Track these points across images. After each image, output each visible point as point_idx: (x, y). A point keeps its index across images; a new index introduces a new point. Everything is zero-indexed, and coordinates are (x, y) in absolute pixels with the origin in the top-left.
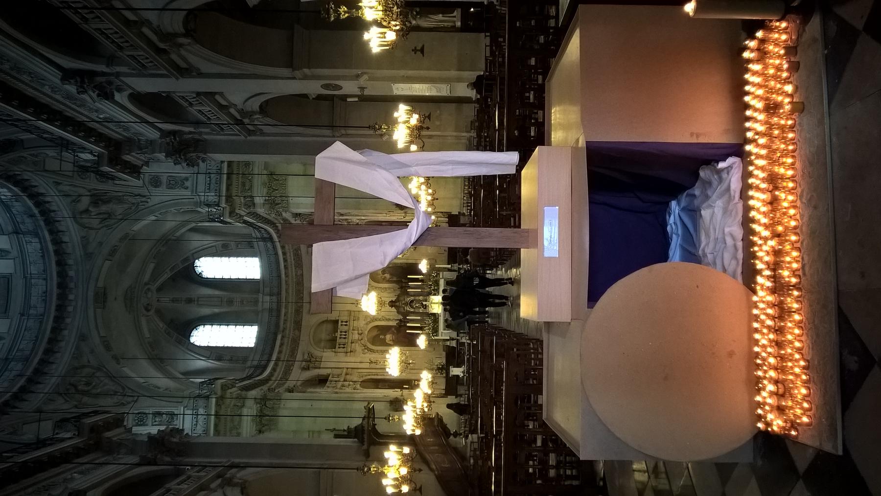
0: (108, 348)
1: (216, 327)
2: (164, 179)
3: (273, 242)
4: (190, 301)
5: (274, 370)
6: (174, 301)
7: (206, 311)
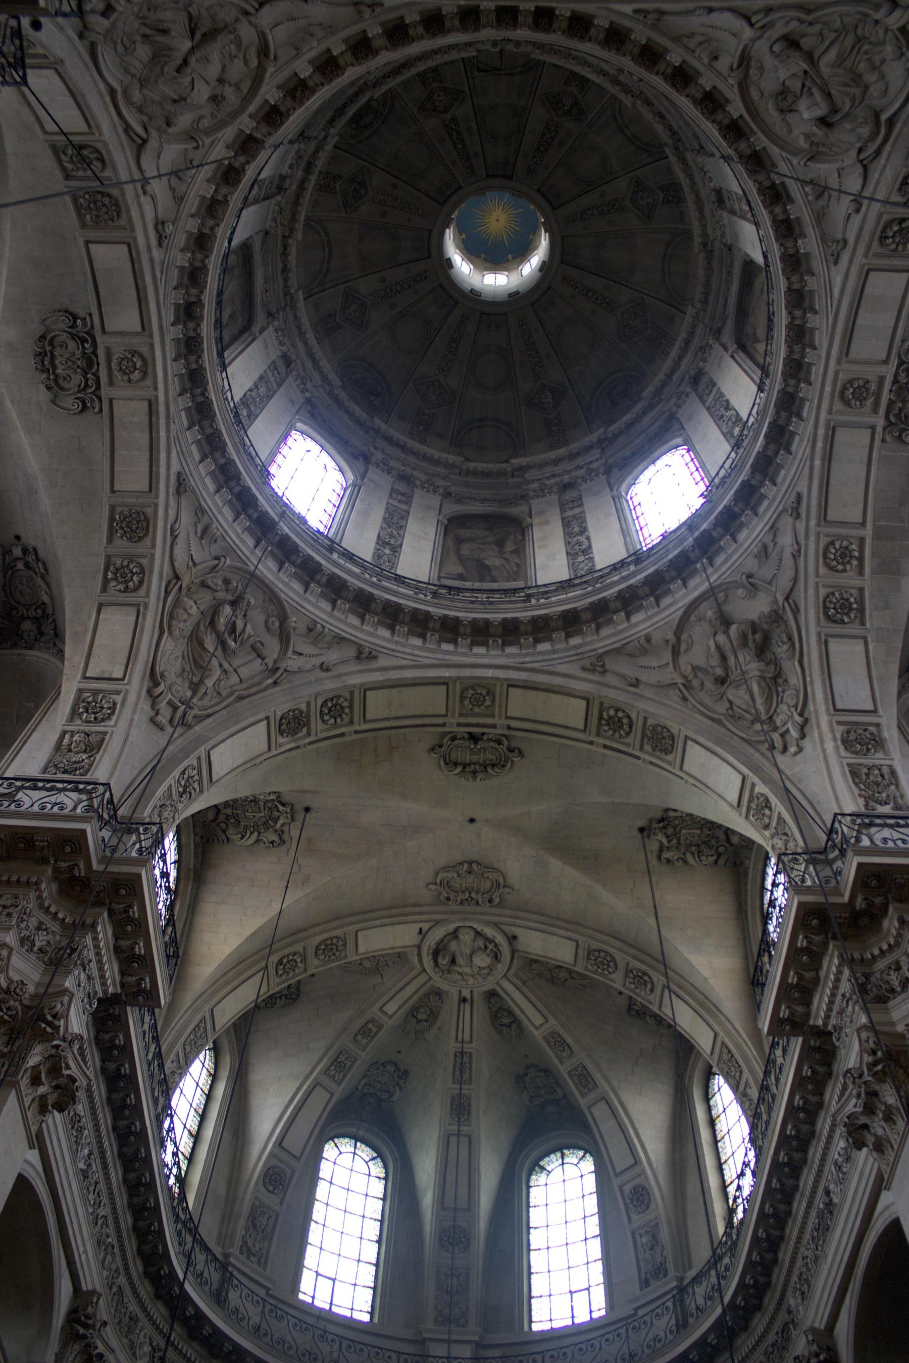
0: (335, 708)
1: (375, 1208)
2: (877, 758)
3: (682, 1325)
4: (460, 1109)
5: (194, 1325)
6: (463, 1063)
7: (426, 1169)
